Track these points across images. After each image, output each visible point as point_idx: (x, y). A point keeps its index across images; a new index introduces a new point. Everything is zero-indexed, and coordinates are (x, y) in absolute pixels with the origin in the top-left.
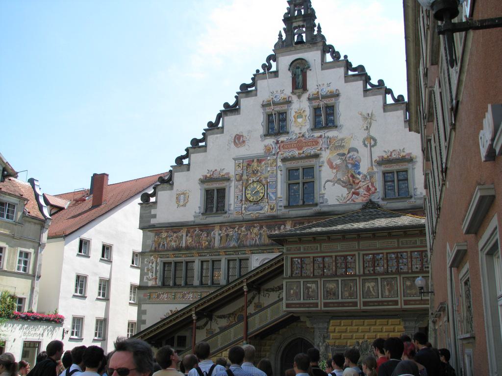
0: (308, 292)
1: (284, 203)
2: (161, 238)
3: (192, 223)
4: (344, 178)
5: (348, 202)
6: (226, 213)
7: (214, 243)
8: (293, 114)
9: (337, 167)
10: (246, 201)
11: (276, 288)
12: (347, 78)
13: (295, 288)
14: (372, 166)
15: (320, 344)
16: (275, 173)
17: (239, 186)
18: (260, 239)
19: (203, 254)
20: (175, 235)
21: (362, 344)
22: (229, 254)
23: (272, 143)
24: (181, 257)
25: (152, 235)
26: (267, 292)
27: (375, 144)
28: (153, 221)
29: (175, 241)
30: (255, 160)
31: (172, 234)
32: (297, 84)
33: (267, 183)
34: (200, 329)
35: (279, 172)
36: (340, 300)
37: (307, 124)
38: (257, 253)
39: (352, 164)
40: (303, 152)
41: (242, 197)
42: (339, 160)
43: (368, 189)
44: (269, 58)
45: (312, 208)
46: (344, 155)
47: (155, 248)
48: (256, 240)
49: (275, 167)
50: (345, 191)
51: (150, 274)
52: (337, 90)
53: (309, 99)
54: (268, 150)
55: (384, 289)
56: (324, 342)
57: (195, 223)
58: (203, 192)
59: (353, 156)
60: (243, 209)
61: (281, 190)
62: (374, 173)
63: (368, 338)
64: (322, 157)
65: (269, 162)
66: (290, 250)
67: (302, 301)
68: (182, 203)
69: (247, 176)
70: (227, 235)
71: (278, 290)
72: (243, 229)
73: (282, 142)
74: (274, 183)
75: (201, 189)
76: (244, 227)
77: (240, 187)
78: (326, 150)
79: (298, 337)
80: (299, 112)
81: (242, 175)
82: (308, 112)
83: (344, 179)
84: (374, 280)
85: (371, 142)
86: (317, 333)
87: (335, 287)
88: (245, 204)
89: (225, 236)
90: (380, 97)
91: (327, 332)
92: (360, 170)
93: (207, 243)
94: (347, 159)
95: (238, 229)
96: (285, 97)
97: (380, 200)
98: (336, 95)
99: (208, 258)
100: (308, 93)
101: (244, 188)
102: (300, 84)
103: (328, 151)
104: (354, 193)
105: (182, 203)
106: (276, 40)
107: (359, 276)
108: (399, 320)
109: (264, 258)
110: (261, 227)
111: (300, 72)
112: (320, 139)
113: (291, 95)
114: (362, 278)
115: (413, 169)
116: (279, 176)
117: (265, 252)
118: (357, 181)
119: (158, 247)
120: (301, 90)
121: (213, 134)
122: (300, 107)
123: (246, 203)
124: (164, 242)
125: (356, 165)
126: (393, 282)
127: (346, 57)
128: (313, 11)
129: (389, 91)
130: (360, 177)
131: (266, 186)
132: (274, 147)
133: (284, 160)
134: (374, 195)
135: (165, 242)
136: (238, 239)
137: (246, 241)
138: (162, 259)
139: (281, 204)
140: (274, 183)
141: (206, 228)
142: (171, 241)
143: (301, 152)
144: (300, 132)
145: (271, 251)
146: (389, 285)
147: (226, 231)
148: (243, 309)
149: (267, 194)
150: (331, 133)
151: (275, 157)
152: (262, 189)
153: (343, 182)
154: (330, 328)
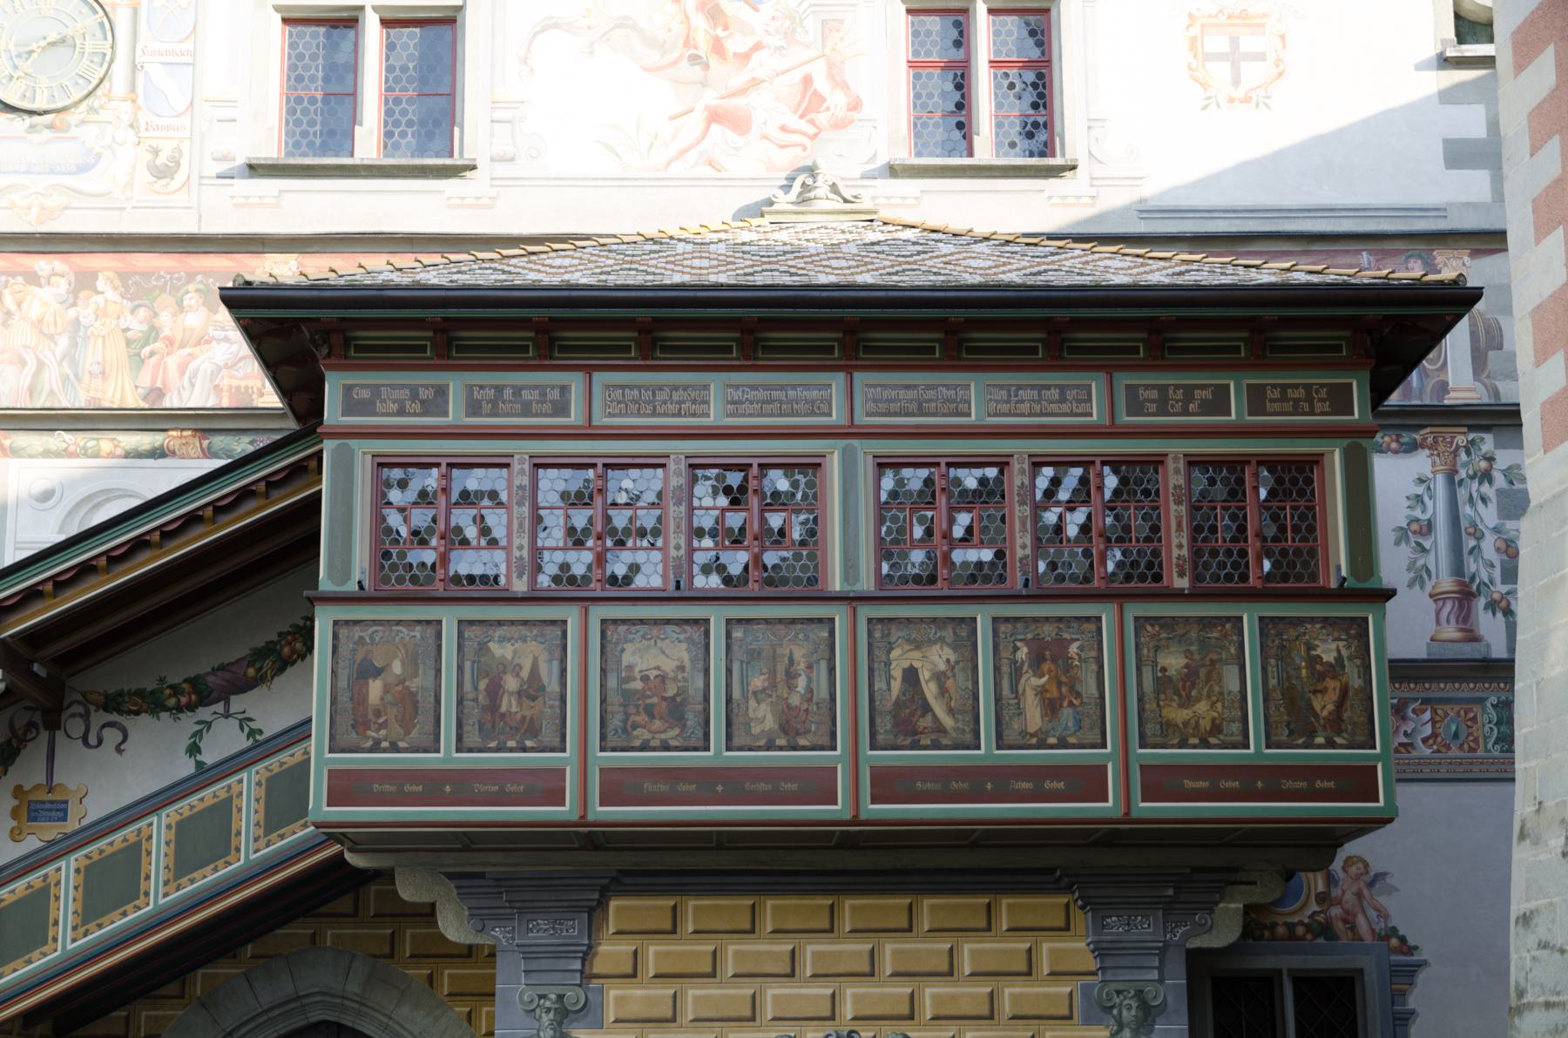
0: (495, 691)
5: (677, 169)
11: (176, 689)
13: (397, 668)
18: (70, 357)
26: (114, 717)
36: (716, 754)
43: (810, 101)
48: (41, 365)
55: (1014, 689)
63: (855, 1019)
66: (366, 408)
67: (447, 756)
71: (191, 707)
79: (315, 1017)
84: (948, 633)
87: (681, 668)
91: (586, 976)
104: (715, 116)
108: (1063, 900)
114: (866, 612)
118: (735, 44)
126: (1073, 649)
146: (1046, 666)
154: (603, 949)
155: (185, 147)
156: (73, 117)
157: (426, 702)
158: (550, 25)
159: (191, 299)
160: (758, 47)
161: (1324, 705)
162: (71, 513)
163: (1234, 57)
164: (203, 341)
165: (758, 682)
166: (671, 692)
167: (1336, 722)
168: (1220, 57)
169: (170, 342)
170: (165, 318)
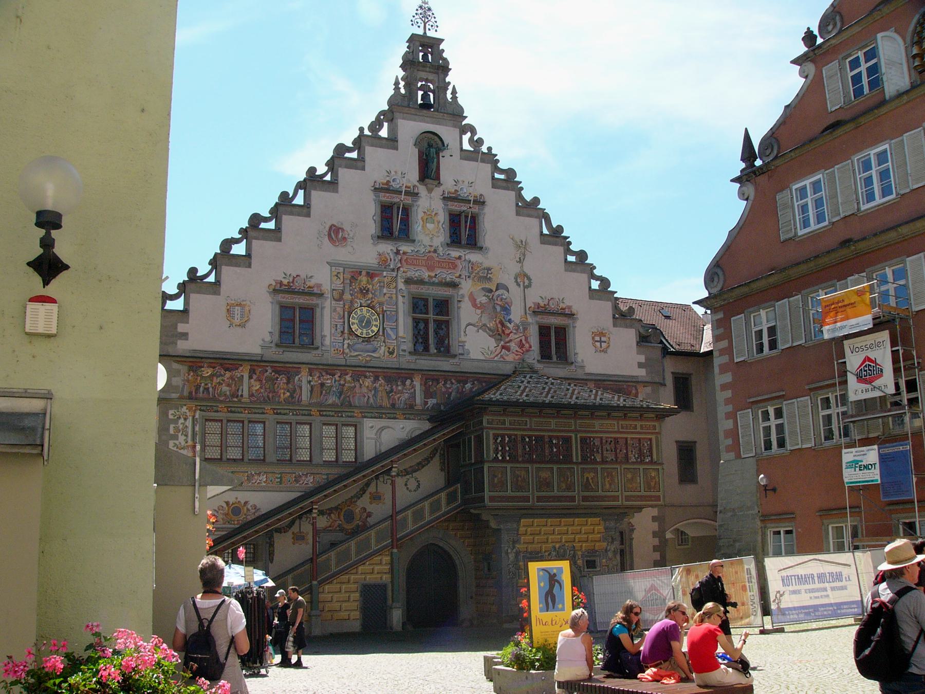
1: (408, 346)
2: (202, 377)
3: (259, 358)
4: (491, 325)
5: (496, 359)
6: (317, 348)
7: (301, 395)
8: (421, 215)
9: (481, 307)
10: (351, 335)
12: (495, 183)
14: (526, 314)
15: (509, 551)
16: (394, 298)
17: (338, 309)
18: (374, 395)
19: (282, 411)
20: (228, 374)
21: (559, 548)
22: (326, 416)
23: (389, 252)
24: (242, 413)
25: (183, 369)
27: (529, 286)
28: (183, 346)
29: (229, 385)
30: (364, 273)
31: (223, 372)
32: (429, 171)
33: (384, 312)
34: (281, 533)
35: (400, 298)
36: (556, 493)
37: (439, 234)
38: (372, 418)
39: (501, 306)
40: (436, 275)
41: (344, 328)
42: (484, 298)
43: (521, 345)
44: (382, 113)
45: (448, 359)
46: (490, 291)
47: (191, 393)
49: (394, 290)
50: (491, 343)
51: (182, 438)
52: (481, 195)
53: (446, 199)
54: (384, 262)
56: (514, 547)
57: (264, 359)
58: (277, 308)
59: (502, 295)
60: (346, 346)
61: (404, 326)
62: (529, 324)
64: (461, 288)
65: (386, 280)
67: (509, 493)
68: (237, 321)
69: (352, 295)
70: (322, 385)
71: (405, 475)
72: (348, 378)
73: (404, 253)
74: (393, 313)
75: (272, 303)
76: (350, 375)
77: (340, 310)
78: (468, 279)
80: (429, 213)
81: (343, 292)
82: (442, 217)
83: (491, 325)
85: (524, 280)
86: (505, 537)
88: (349, 339)
89: (319, 385)
90: (535, 221)
92: (511, 317)
93: (288, 394)
94: (495, 297)
95: (339, 377)
96: (409, 185)
97: (535, 361)
98: (480, 202)
99: (290, 417)
100: (442, 188)
101: (346, 313)
102: (433, 171)
103: (470, 282)
104: (503, 347)
105: (237, 321)
106: (393, 92)
107: (576, 463)
109: (382, 426)
110: (376, 378)
111: (435, 156)
112: (459, 261)
113: (417, 184)
115: (574, 327)
116: (400, 304)
117: (384, 416)
118: (507, 332)
119: (196, 393)
120: (436, 182)
121: (291, 214)
122: (430, 206)
123: (351, 337)
124: (206, 384)
125: (506, 309)
126: (614, 473)
127: (490, 149)
128: (445, 60)
129: (547, 217)
130: (511, 326)
131: (381, 316)
132: (392, 258)
133: (408, 281)
134: (529, 353)
135: (210, 385)
136: (341, 393)
137: (353, 397)
138: (204, 413)
139: (404, 347)
140: (393, 313)
141: (288, 370)
142: (220, 384)
143: (433, 275)
144: (431, 244)
145: (392, 416)
147: (319, 377)
148: (352, 500)
149: (384, 329)
150: (474, 257)
151: (394, 274)
152: (376, 320)
153: (490, 330)
155: (395, 348)
156: (371, 340)
157: (505, 482)
158: (469, 324)
159: (399, 383)
160: (511, 332)
161: (653, 484)
162: (378, 430)
163: (601, 342)
164: (402, 393)
165: (562, 479)
166: (548, 481)
167: (654, 487)
168: (597, 341)
169: (395, 392)
170: (394, 387)
